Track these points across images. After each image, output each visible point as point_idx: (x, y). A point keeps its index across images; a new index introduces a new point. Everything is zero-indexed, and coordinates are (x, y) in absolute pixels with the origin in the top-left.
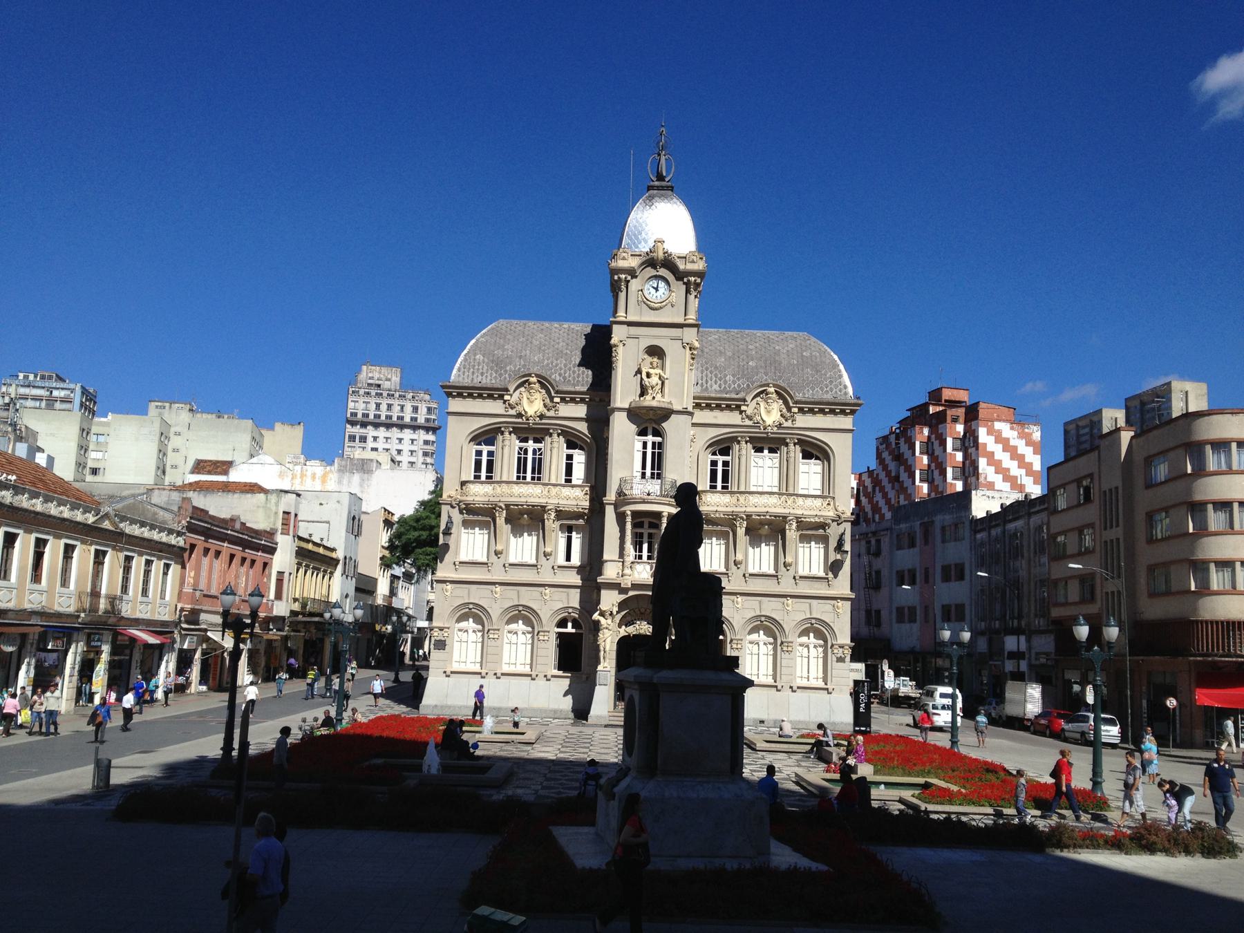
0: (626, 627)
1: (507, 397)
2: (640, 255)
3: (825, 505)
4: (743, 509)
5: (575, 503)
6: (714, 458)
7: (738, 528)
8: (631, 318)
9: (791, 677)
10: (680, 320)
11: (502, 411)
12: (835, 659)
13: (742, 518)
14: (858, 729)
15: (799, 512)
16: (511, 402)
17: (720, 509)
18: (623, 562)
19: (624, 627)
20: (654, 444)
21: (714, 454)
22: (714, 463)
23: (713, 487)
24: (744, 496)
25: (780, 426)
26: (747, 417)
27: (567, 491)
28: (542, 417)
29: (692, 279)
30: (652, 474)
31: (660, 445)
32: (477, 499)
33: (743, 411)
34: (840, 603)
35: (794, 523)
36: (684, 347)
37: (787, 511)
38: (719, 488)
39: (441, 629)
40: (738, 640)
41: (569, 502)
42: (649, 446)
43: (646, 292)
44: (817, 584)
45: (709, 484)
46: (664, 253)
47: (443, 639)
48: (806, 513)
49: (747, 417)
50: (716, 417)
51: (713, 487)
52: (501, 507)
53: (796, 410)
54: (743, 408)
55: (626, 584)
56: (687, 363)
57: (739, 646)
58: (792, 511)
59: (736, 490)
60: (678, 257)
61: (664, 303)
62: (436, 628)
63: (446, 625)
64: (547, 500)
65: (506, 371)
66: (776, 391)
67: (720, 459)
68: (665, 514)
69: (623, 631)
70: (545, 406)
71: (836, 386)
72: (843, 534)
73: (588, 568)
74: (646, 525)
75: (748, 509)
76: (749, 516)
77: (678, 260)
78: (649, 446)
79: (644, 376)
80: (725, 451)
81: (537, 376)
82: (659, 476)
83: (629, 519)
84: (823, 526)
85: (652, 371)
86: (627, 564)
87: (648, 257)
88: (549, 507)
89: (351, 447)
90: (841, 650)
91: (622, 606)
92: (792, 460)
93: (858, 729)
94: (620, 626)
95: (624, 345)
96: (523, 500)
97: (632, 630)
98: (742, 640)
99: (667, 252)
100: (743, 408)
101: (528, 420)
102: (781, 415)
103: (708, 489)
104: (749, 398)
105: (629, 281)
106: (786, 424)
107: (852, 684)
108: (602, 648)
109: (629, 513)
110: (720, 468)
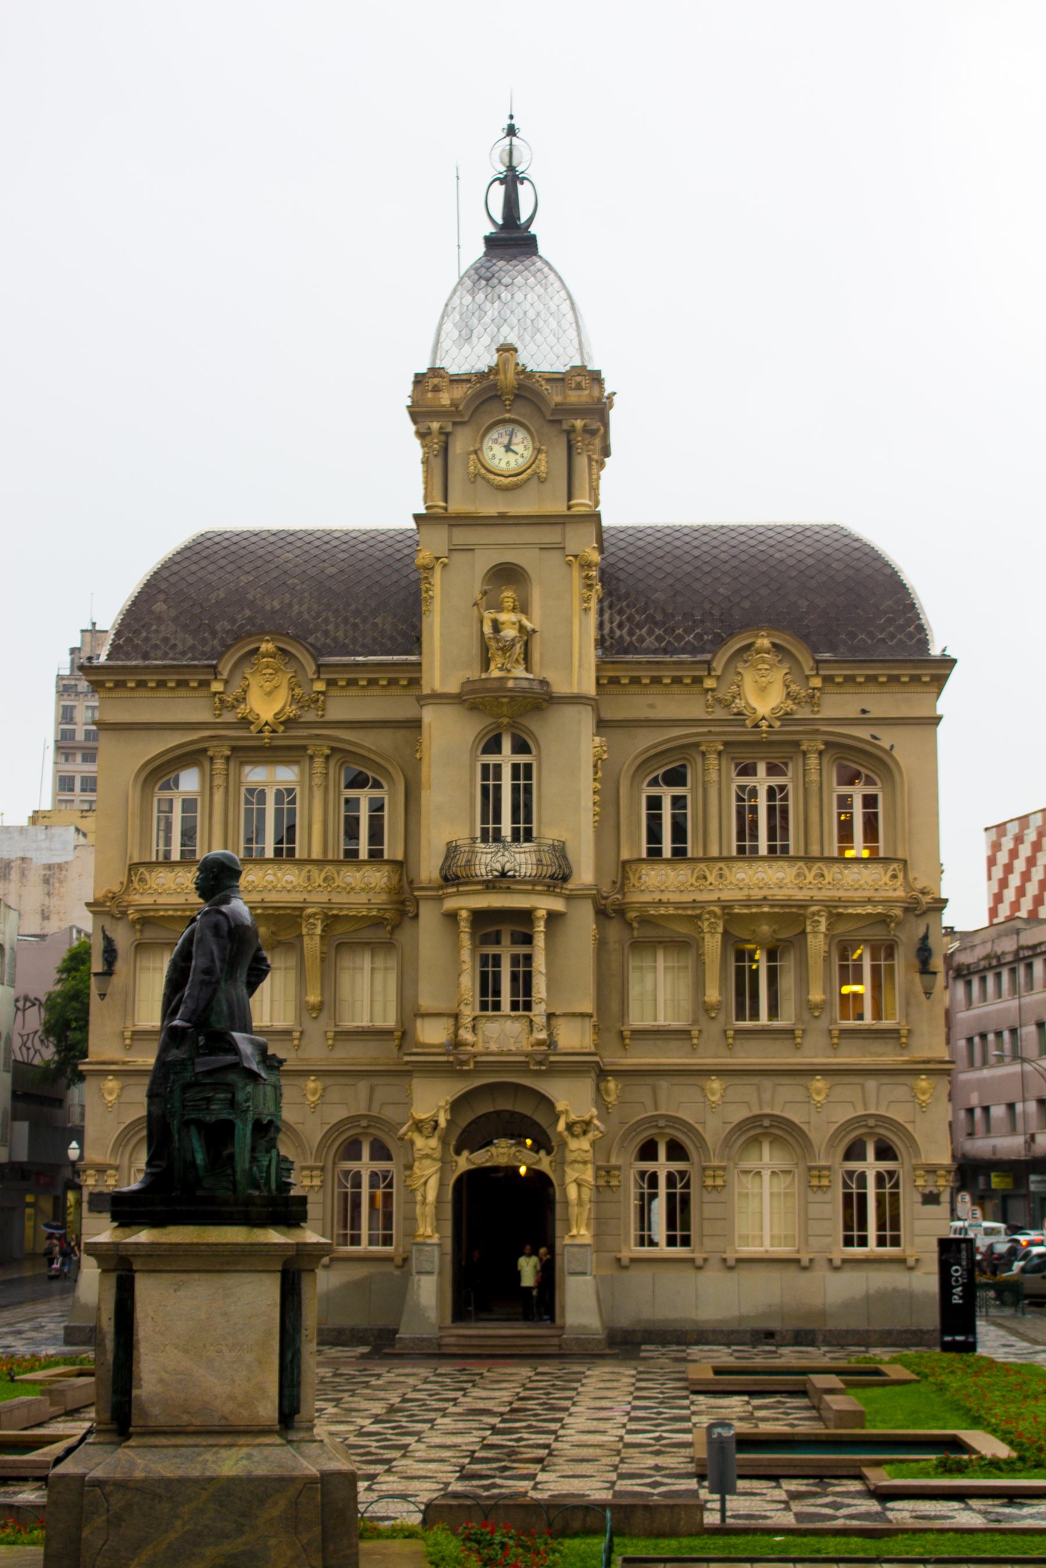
0: (472, 1152)
1: (217, 687)
2: (468, 381)
3: (886, 878)
4: (714, 897)
5: (363, 898)
6: (654, 791)
7: (707, 936)
8: (457, 506)
9: (830, 1239)
10: (560, 508)
11: (206, 716)
12: (920, 1199)
13: (712, 913)
14: (948, 1339)
16: (224, 697)
17: (665, 898)
18: (456, 1017)
19: (465, 1153)
20: (515, 767)
21: (654, 783)
22: (655, 803)
23: (655, 853)
24: (816, 867)
25: (786, 718)
27: (351, 876)
28: (289, 723)
29: (579, 424)
30: (515, 832)
31: (528, 767)
32: (161, 900)
33: (708, 690)
34: (923, 1082)
35: (823, 920)
36: (569, 564)
38: (667, 852)
39: (101, 1170)
40: (715, 1169)
41: (353, 898)
42: (507, 773)
43: (487, 454)
44: (877, 1046)
45: (644, 845)
46: (518, 374)
49: (719, 701)
50: (652, 706)
51: (655, 853)
53: (817, 682)
57: (719, 1182)
59: (701, 855)
60: (548, 380)
63: (108, 1160)
64: (305, 896)
65: (214, 633)
66: (774, 645)
67: (667, 794)
68: (541, 913)
69: (464, 1162)
70: (294, 700)
71: (901, 628)
72: (925, 938)
73: (398, 1034)
74: (506, 939)
75: (726, 895)
76: (726, 907)
77: (546, 386)
78: (507, 773)
79: (488, 629)
80: (675, 777)
82: (528, 837)
83: (465, 926)
84: (883, 920)
85: (504, 617)
86: (466, 1021)
87: (485, 383)
88: (309, 911)
89: (66, 801)
90: (931, 1178)
91: (457, 1106)
92: (814, 788)
93: (948, 1339)
94: (458, 1152)
95: (445, 566)
97: (482, 1158)
98: (724, 1168)
99: (523, 372)
100: (709, 683)
101: (261, 731)
102: (788, 694)
103: (644, 855)
104: (718, 665)
105: (447, 435)
106: (804, 713)
107: (935, 1247)
108: (419, 1198)
109: (464, 914)
110: (667, 812)
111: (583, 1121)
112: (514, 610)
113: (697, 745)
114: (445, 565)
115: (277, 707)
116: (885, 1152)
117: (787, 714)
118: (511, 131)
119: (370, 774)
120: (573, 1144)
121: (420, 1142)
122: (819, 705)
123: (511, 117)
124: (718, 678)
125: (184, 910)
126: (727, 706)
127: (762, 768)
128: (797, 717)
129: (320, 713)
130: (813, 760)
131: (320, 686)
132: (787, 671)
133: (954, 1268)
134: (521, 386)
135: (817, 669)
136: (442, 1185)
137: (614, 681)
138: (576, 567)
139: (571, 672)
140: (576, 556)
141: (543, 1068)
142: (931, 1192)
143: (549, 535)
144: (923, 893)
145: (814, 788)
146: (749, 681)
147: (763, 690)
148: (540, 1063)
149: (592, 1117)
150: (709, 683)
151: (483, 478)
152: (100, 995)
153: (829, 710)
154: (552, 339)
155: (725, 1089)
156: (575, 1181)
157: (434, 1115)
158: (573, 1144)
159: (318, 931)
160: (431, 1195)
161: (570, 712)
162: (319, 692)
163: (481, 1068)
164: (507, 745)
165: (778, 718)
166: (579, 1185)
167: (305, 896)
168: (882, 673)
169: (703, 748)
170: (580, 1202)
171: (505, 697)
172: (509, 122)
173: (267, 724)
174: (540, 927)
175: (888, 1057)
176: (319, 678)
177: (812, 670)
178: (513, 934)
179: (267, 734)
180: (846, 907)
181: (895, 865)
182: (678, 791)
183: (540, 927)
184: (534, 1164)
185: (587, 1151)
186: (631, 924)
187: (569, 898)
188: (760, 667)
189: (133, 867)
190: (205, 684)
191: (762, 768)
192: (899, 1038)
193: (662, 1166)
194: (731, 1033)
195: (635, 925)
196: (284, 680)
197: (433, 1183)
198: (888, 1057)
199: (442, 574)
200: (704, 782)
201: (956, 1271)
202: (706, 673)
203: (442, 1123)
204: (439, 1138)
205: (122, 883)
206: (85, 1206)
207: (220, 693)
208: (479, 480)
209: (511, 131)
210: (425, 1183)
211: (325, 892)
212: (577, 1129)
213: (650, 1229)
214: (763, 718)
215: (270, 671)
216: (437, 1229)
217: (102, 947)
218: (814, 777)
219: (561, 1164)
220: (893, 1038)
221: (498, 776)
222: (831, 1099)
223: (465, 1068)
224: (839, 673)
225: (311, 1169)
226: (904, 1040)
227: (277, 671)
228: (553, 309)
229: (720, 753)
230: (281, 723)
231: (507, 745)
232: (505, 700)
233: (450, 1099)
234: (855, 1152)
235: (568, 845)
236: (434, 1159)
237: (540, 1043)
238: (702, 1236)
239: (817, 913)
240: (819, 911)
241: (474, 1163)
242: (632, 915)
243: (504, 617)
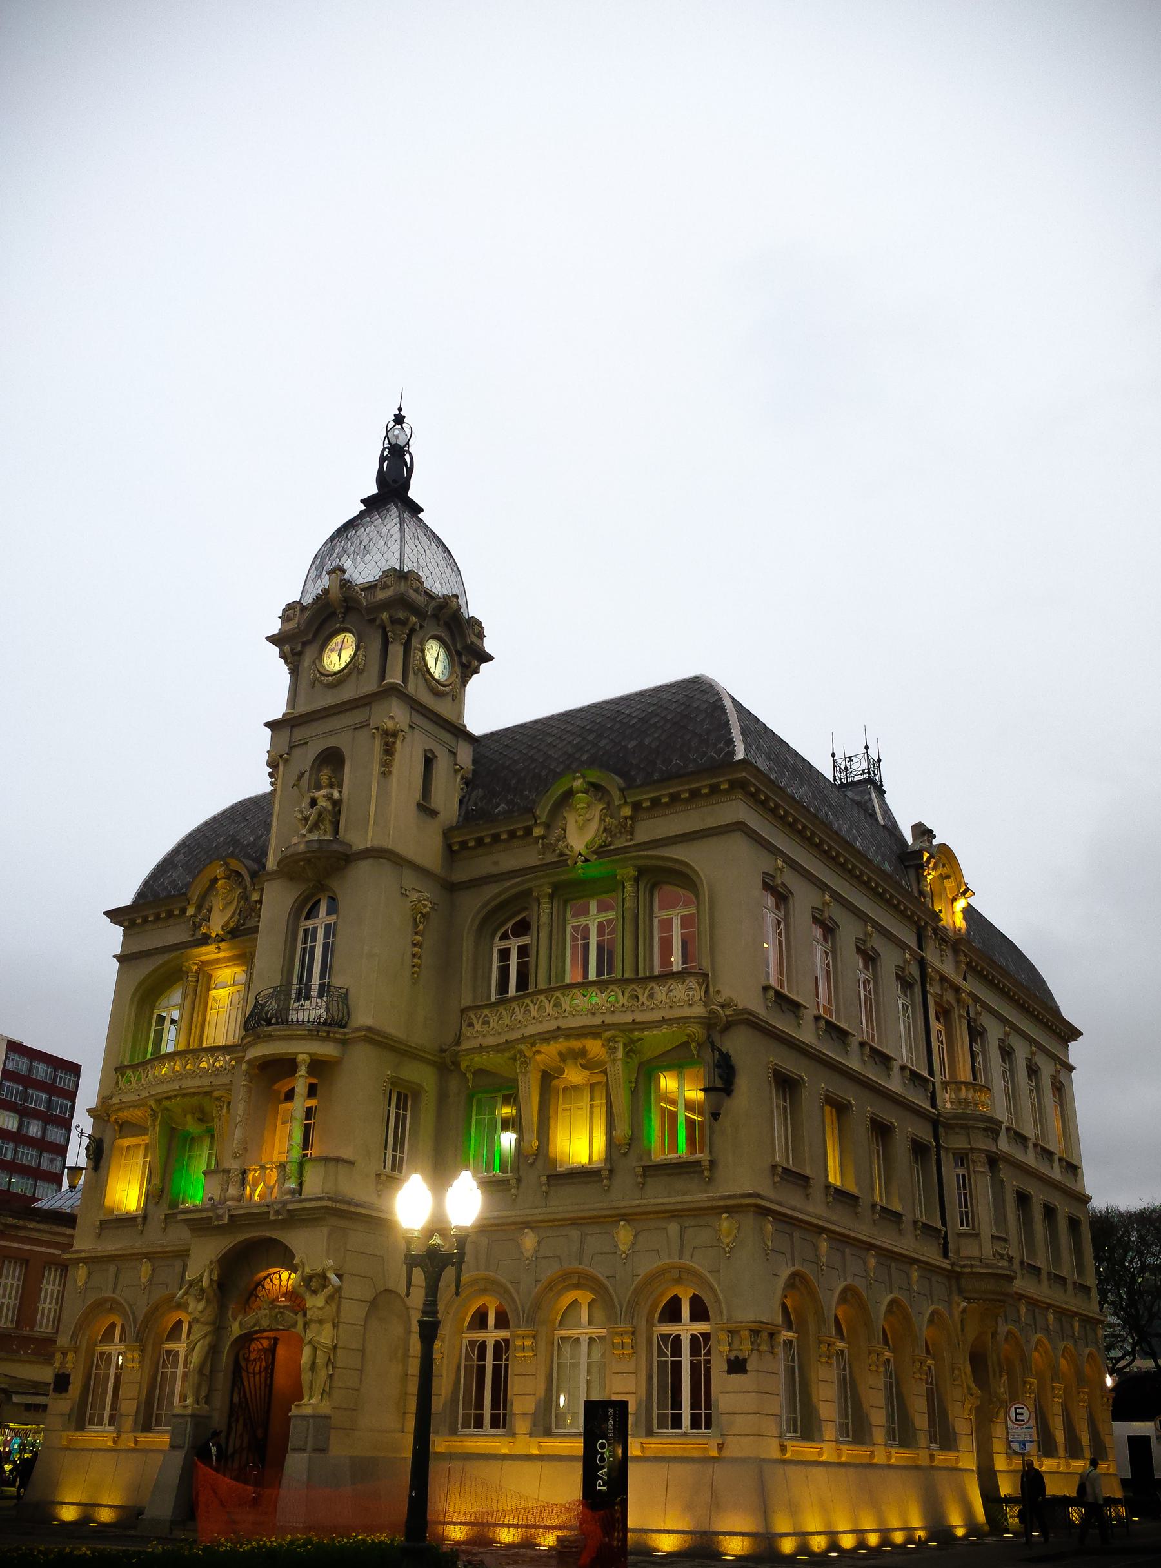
6: (504, 944)
15: (628, 1018)
19: (240, 1317)
21: (504, 937)
29: (385, 616)
30: (322, 986)
34: (725, 1223)
35: (621, 1046)
37: (597, 1020)
48: (640, 1018)
53: (627, 811)
55: (219, 1217)
56: (376, 766)
58: (609, 1019)
61: (345, 671)
67: (514, 944)
94: (235, 1319)
96: (175, 1086)
100: (538, 831)
102: (605, 830)
104: (543, 813)
106: (620, 843)
111: (318, 1275)
112: (331, 785)
113: (529, 892)
114: (287, 761)
116: (700, 1312)
117: (601, 847)
118: (399, 419)
122: (632, 834)
123: (400, 409)
126: (554, 851)
127: (593, 906)
128: (611, 847)
130: (629, 887)
132: (604, 806)
133: (600, 1442)
134: (346, 599)
135: (625, 797)
136: (213, 1351)
137: (464, 845)
138: (378, 736)
139: (367, 833)
141: (280, 1217)
142: (737, 1357)
143: (358, 716)
144: (723, 1006)
145: (629, 916)
146: (572, 821)
147: (581, 828)
148: (277, 1213)
149: (324, 1270)
153: (641, 836)
154: (378, 556)
155: (539, 1243)
161: (364, 868)
162: (256, 902)
163: (237, 1223)
165: (594, 852)
166: (315, 1349)
167: (212, 1079)
168: (682, 788)
169: (535, 894)
170: (313, 1366)
171: (302, 860)
172: (398, 412)
174: (302, 1071)
175: (693, 1195)
176: (254, 889)
177: (620, 800)
180: (642, 1030)
181: (692, 979)
182: (523, 940)
183: (302, 1071)
185: (321, 1309)
186: (465, 1074)
187: (344, 1042)
188: (578, 806)
190: (183, 911)
191: (593, 906)
192: (702, 1172)
193: (491, 1336)
194: (544, 1179)
195: (470, 1076)
198: (693, 1195)
199: (284, 768)
200: (538, 926)
201: (602, 1446)
202: (533, 822)
203: (205, 1283)
204: (208, 1301)
208: (317, 684)
209: (399, 419)
211: (230, 1075)
212: (314, 1284)
213: (505, 1409)
218: (629, 904)
219: (306, 1325)
220: (695, 1172)
221: (314, 939)
222: (637, 1248)
223: (221, 1223)
224: (645, 797)
226: (706, 1173)
228: (385, 531)
229: (551, 897)
232: (302, 863)
233: (214, 1258)
234: (672, 1313)
235: (352, 992)
236: (202, 1323)
237: (292, 1192)
238: (140, 1383)
241: (246, 1329)
242: (463, 1065)
243: (319, 794)
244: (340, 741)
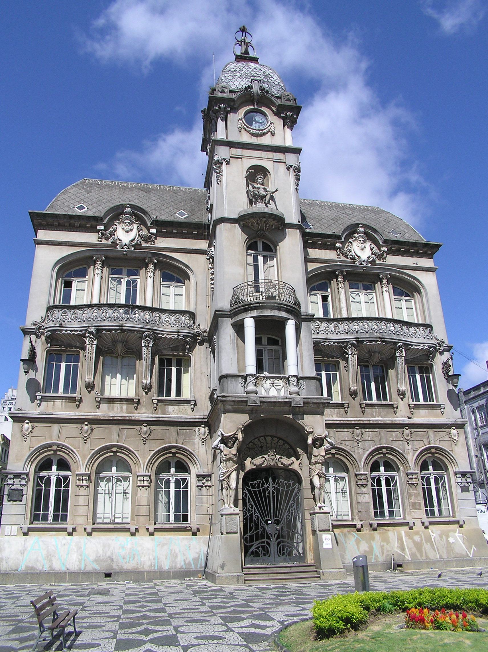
13: (352, 345)
19: (249, 459)
25: (373, 262)
26: (343, 254)
36: (288, 169)
47: (20, 488)
52: (91, 333)
54: (338, 245)
61: (265, 131)
62: (11, 474)
81: (132, 206)
91: (247, 429)
101: (123, 248)
102: (372, 254)
115: (132, 238)
119: (175, 275)
120: (315, 451)
121: (226, 450)
124: (342, 243)
125: (77, 331)
129: (152, 243)
131: (154, 231)
140: (291, 166)
150: (338, 245)
151: (245, 130)
152: (25, 372)
156: (317, 474)
157: (235, 434)
158: (315, 451)
159: (151, 345)
160: (233, 485)
162: (152, 234)
164: (260, 246)
173: (126, 245)
178: (269, 339)
179: (125, 249)
184: (290, 465)
189: (49, 309)
196: (135, 226)
197: (234, 475)
205: (42, 317)
206: (5, 498)
207: (101, 230)
210: (229, 477)
214: (364, 261)
215: (129, 221)
216: (236, 505)
217: (29, 348)
225: (144, 476)
227: (131, 223)
230: (133, 246)
231: (260, 246)
239: (400, 347)
240: (402, 346)
244: (268, 165)
